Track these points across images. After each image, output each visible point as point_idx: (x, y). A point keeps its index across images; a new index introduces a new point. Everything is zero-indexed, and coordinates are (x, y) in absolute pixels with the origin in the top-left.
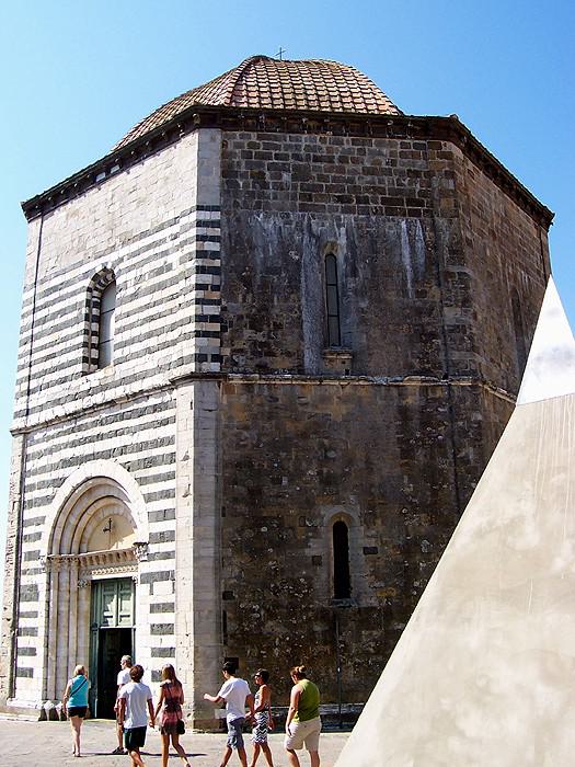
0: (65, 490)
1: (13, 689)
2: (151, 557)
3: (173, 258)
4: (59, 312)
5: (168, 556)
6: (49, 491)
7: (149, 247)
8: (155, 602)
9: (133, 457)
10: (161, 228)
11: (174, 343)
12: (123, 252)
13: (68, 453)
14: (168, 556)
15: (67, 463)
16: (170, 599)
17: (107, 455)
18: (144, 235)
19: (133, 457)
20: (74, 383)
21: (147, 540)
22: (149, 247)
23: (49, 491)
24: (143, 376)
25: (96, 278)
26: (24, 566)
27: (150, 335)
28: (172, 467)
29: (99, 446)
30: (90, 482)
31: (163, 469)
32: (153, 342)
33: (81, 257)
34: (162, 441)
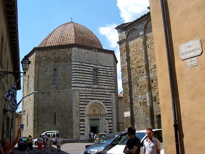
2: (108, 116)
4: (86, 71)
5: (110, 116)
6: (86, 103)
7: (105, 69)
9: (104, 101)
10: (107, 67)
12: (100, 67)
13: (91, 97)
14: (110, 116)
15: (89, 99)
16: (112, 122)
18: (104, 66)
19: (104, 101)
20: (91, 85)
22: (105, 69)
23: (86, 103)
24: (105, 89)
27: (106, 83)
28: (111, 104)
29: (97, 98)
32: (107, 84)
33: (90, 63)
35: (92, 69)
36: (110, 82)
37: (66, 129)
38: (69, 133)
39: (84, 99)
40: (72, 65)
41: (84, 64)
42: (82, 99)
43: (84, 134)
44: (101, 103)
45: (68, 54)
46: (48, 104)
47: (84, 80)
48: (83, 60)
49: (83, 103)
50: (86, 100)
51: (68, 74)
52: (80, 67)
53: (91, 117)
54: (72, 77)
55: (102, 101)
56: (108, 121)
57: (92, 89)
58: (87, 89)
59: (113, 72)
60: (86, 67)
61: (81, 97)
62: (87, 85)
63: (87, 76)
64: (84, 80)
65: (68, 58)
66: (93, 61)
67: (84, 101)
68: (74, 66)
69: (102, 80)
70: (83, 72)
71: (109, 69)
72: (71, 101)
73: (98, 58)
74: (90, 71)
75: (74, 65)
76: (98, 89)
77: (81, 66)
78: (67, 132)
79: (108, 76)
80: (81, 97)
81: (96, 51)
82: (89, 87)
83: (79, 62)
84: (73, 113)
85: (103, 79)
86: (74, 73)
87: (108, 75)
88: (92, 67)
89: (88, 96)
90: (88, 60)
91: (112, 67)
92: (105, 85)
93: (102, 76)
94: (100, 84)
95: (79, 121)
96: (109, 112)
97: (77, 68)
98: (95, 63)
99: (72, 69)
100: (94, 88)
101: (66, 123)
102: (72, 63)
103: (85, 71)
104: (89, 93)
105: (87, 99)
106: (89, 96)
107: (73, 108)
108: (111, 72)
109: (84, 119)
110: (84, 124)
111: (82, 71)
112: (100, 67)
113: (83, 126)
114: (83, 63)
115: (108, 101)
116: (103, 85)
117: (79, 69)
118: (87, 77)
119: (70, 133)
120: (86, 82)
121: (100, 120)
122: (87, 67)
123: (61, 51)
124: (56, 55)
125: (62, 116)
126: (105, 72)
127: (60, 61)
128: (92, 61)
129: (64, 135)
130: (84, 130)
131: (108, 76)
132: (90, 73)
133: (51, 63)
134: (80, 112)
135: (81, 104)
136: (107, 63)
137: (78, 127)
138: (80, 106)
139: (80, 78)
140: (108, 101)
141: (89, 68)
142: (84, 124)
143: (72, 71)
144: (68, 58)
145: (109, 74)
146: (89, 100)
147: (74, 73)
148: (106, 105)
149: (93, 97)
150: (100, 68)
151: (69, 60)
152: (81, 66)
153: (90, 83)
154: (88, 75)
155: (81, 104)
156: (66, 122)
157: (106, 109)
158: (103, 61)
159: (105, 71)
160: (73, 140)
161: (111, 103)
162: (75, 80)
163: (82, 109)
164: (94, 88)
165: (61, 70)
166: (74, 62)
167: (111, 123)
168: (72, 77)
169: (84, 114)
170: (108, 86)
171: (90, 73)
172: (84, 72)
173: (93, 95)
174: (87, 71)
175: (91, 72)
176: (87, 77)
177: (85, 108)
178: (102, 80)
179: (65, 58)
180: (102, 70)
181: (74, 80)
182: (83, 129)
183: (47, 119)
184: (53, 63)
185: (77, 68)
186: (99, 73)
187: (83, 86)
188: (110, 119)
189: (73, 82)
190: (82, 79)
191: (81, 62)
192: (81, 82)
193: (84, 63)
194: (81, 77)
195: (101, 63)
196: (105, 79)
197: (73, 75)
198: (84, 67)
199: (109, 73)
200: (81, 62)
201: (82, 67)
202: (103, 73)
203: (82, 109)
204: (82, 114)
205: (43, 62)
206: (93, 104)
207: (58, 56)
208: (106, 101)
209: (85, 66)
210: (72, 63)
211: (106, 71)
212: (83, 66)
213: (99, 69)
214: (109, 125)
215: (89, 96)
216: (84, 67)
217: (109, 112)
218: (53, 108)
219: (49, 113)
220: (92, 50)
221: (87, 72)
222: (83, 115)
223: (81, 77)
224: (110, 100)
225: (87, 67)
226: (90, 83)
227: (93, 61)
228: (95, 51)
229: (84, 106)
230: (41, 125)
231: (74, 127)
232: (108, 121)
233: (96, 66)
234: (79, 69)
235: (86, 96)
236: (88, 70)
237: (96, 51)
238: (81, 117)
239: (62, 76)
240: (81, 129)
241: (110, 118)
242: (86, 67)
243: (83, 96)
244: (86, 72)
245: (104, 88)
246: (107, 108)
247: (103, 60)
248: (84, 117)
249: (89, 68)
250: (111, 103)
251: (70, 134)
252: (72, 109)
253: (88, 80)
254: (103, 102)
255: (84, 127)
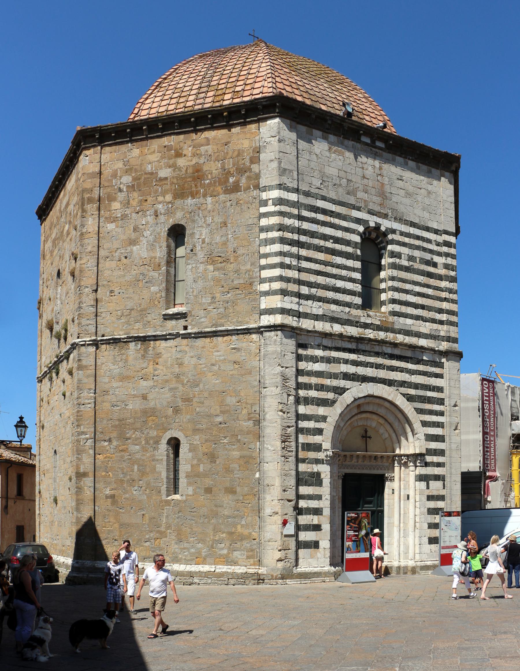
0: (348, 398)
1: (297, 559)
2: (427, 464)
3: (440, 260)
4: (332, 237)
5: (439, 465)
6: (330, 396)
7: (418, 238)
8: (430, 494)
9: (412, 392)
10: (427, 229)
11: (441, 322)
12: (396, 226)
13: (351, 369)
14: (439, 465)
15: (346, 376)
16: (442, 492)
17: (390, 383)
18: (413, 225)
19: (412, 392)
20: (355, 312)
21: (424, 452)
22: (418, 238)
23: (330, 396)
24: (419, 335)
25: (367, 228)
26: (301, 455)
27: (423, 307)
29: (382, 374)
30: (371, 399)
31: (436, 407)
33: (351, 200)
34: (434, 387)
35: (359, 234)
36: (437, 304)
37: (228, 517)
38: (242, 538)
39: (319, 374)
40: (264, 203)
41: (321, 204)
42: (310, 374)
43: (316, 545)
44: (401, 402)
45: (240, 153)
46: (144, 397)
47: (321, 280)
48: (317, 182)
49: (313, 393)
50: (328, 382)
51: (240, 251)
52: (301, 218)
53: (347, 467)
54: (263, 262)
55: (403, 390)
56: (428, 488)
57: (360, 330)
58: (337, 328)
59: (453, 257)
60: (328, 219)
61: (302, 365)
62: (333, 307)
63: (339, 266)
64: (321, 280)
65: (242, 171)
66: (365, 196)
67: (320, 388)
68: (271, 208)
69: (407, 292)
70: (316, 241)
71: (438, 244)
72: (256, 383)
73: (386, 180)
74: (348, 243)
75: (270, 202)
76: (386, 330)
77: (305, 213)
78: (231, 534)
79: (430, 275)
80: (302, 365)
81: (380, 148)
82: (346, 317)
83: (297, 191)
84: (262, 443)
85: (408, 287)
86: (273, 241)
87: (431, 269)
88: (358, 221)
89: (337, 361)
90: (340, 185)
91: (446, 232)
92: (417, 318)
93: (407, 269)
94: (397, 308)
95: (293, 482)
96: (434, 445)
97: (288, 222)
98: (371, 206)
99: (264, 222)
100: (366, 326)
101: (231, 491)
102: (264, 196)
103: (325, 237)
104: (344, 350)
105: (335, 376)
106: (346, 362)
107: (268, 417)
108: (447, 255)
109: (318, 474)
110: (319, 497)
111: (313, 234)
112: (396, 226)
113: (313, 504)
114: (316, 196)
115: (430, 394)
116: (411, 317)
117: (296, 223)
118: (335, 271)
119: (248, 537)
120: (330, 295)
121: (387, 484)
122: (336, 221)
123: (208, 142)
124: (181, 162)
125: (212, 457)
126: (417, 254)
127: (203, 186)
128: (360, 195)
129: (222, 549)
130: (317, 528)
131: (430, 275)
132: (349, 249)
133: (160, 199)
134: (302, 439)
135: (307, 401)
136: (426, 215)
137: (290, 511)
138: (302, 409)
139: (300, 270)
140: (430, 394)
141: (344, 224)
142: (319, 497)
143: (263, 236)
144: (242, 171)
145: (435, 265)
146: (342, 383)
147: (273, 241)
148: (420, 411)
149: (361, 371)
150: (394, 231)
151: (249, 178)
152: (305, 213)
153: (348, 298)
154: (339, 260)
155: (307, 401)
156: (228, 485)
157: (422, 431)
158: (407, 201)
159: (418, 248)
160: (262, 571)
161: (441, 402)
162: (281, 278)
163: (311, 424)
164: (366, 326)
165: (205, 232)
166: (270, 188)
167: (441, 498)
168: (263, 262)
169: (318, 448)
170: (434, 321)
171: (349, 249)
172: (322, 243)
173: (362, 358)
174: (337, 240)
175: (355, 245)
176: (335, 271)
177: (324, 419)
178: (407, 292)
179: (229, 174)
180: (404, 244)
181: (271, 280)
182: (315, 520)
183: (136, 467)
184: (169, 197)
185: (288, 222)
186: (393, 254)
187: (315, 311)
188: (437, 478)
189: (265, 287)
190: (312, 278)
191: (307, 194)
192: (305, 290)
193: (324, 198)
194: (305, 264)
195: (401, 208)
196: (417, 289)
197: (266, 256)
198: (321, 217)
199: (436, 259)
200: (307, 194)
201: (313, 215)
202: (411, 258)
203: (311, 424)
204: (308, 447)
205: (121, 196)
206: (359, 406)
207: (194, 162)
208: (421, 393)
209: (324, 212)
210: (264, 196)
211: (425, 250)
212: (316, 212)
213: (390, 237)
214: (432, 504)
215: (346, 362)
216: (321, 217)
217: (434, 445)
218: (166, 417)
219: (147, 442)
220: (358, 140)
221: (338, 247)
222: (312, 455)
223: (305, 264)
224: (440, 389)
225: (336, 221)
226: (348, 298)
227: (365, 196)
228: (372, 145)
229: (321, 411)
230: (113, 497)
231: (268, 511)
232: (428, 488)
233: (379, 220)
234: (296, 223)
235: (328, 360)
236: (339, 234)
237: (380, 148)
238: (303, 461)
239: (213, 262)
240: (304, 520)
241: (437, 471)
242: (328, 219)
243: (314, 359)
244: (329, 244)
245: (414, 329)
246: (425, 424)
247: (408, 195)
248: (317, 461)
249: (344, 224)
250: (441, 402)
251: (246, 544)
252: (258, 422)
253: (340, 284)
254: (410, 398)
255: (317, 512)
